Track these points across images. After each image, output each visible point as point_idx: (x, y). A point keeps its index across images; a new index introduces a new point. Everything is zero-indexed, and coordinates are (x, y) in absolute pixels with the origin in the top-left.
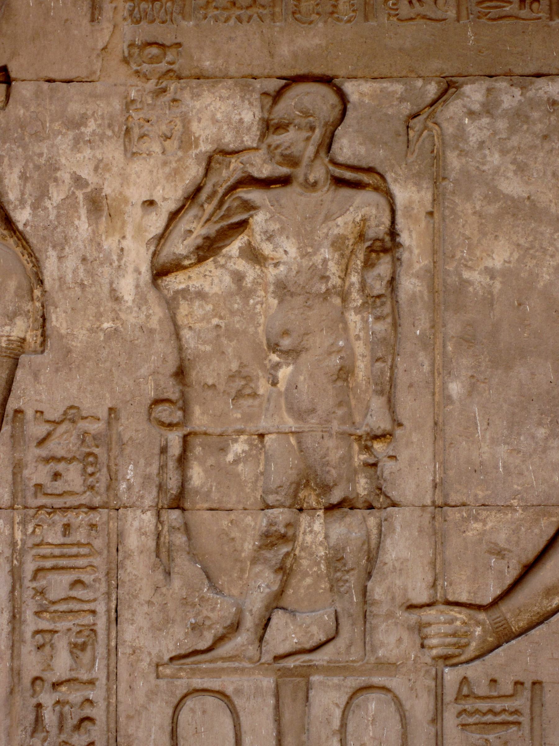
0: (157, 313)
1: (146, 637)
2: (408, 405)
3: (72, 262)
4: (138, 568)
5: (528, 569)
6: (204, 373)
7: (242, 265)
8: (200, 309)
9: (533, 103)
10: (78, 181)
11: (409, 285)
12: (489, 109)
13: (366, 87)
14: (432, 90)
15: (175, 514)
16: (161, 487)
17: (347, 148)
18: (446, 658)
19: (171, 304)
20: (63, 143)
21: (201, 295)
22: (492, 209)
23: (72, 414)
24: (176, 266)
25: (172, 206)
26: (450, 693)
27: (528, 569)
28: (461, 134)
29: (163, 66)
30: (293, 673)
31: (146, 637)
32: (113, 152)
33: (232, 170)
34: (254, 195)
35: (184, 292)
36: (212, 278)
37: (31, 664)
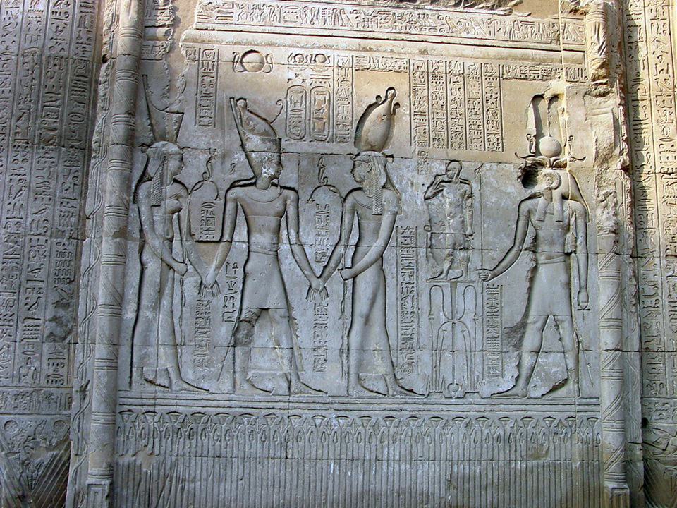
0: (425, 207)
1: (424, 274)
2: (477, 229)
3: (408, 196)
4: (422, 260)
5: (500, 263)
6: (434, 220)
7: (441, 198)
8: (434, 207)
9: (500, 169)
10: (409, 179)
11: (476, 205)
12: (490, 169)
13: (467, 163)
14: (480, 165)
15: (429, 249)
16: (427, 244)
17: (462, 175)
18: (484, 280)
19: (428, 206)
20: (405, 171)
21: (433, 204)
22: (491, 190)
23: (408, 228)
24: (429, 198)
25: (428, 186)
26: (485, 287)
27: (500, 263)
28: (485, 174)
29: (425, 156)
30: (454, 283)
31: (424, 274)
32: (416, 173)
33: (440, 178)
34: (444, 184)
35: (430, 203)
36: (435, 201)
37: (401, 279)
